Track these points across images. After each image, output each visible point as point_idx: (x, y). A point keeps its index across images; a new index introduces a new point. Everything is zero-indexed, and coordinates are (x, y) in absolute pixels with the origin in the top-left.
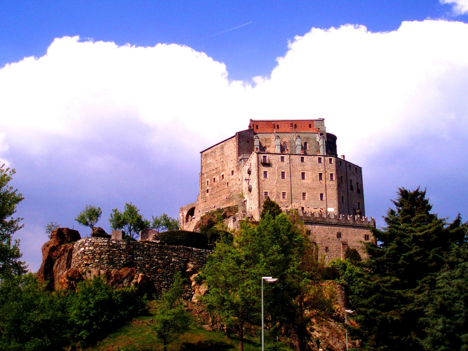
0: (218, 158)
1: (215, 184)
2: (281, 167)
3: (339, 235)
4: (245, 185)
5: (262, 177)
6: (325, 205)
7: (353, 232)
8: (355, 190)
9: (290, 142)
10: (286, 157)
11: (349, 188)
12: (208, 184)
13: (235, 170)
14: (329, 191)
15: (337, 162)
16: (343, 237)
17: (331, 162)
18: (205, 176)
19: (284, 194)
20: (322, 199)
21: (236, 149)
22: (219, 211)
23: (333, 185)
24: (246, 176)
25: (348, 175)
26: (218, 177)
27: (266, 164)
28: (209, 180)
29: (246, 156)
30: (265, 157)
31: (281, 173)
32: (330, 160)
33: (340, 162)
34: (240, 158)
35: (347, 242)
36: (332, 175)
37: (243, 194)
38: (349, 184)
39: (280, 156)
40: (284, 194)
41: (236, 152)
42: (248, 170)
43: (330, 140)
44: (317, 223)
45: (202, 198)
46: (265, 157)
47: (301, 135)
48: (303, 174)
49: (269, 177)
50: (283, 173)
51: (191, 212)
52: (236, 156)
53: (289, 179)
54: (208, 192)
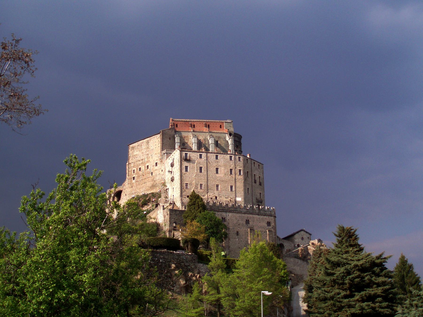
0: (144, 151)
1: (141, 173)
2: (199, 163)
3: (247, 222)
4: (168, 177)
5: (184, 171)
6: (234, 195)
7: (258, 219)
8: (258, 183)
10: (204, 155)
11: (253, 181)
12: (134, 172)
13: (158, 162)
14: (238, 184)
15: (244, 160)
17: (239, 160)
18: (132, 165)
19: (201, 185)
20: (231, 190)
21: (160, 145)
22: (145, 196)
23: (240, 178)
24: (169, 168)
25: (253, 171)
26: (143, 167)
27: (187, 160)
28: (135, 169)
29: (168, 151)
30: (186, 154)
31: (199, 168)
32: (239, 158)
33: (247, 160)
34: (163, 152)
35: (253, 228)
37: (165, 183)
38: (253, 178)
39: (199, 154)
40: (201, 185)
41: (160, 147)
42: (171, 164)
43: (237, 139)
44: (230, 212)
45: (128, 184)
46: (186, 154)
48: (217, 169)
49: (189, 170)
52: (159, 151)
53: (206, 173)
54: (134, 179)
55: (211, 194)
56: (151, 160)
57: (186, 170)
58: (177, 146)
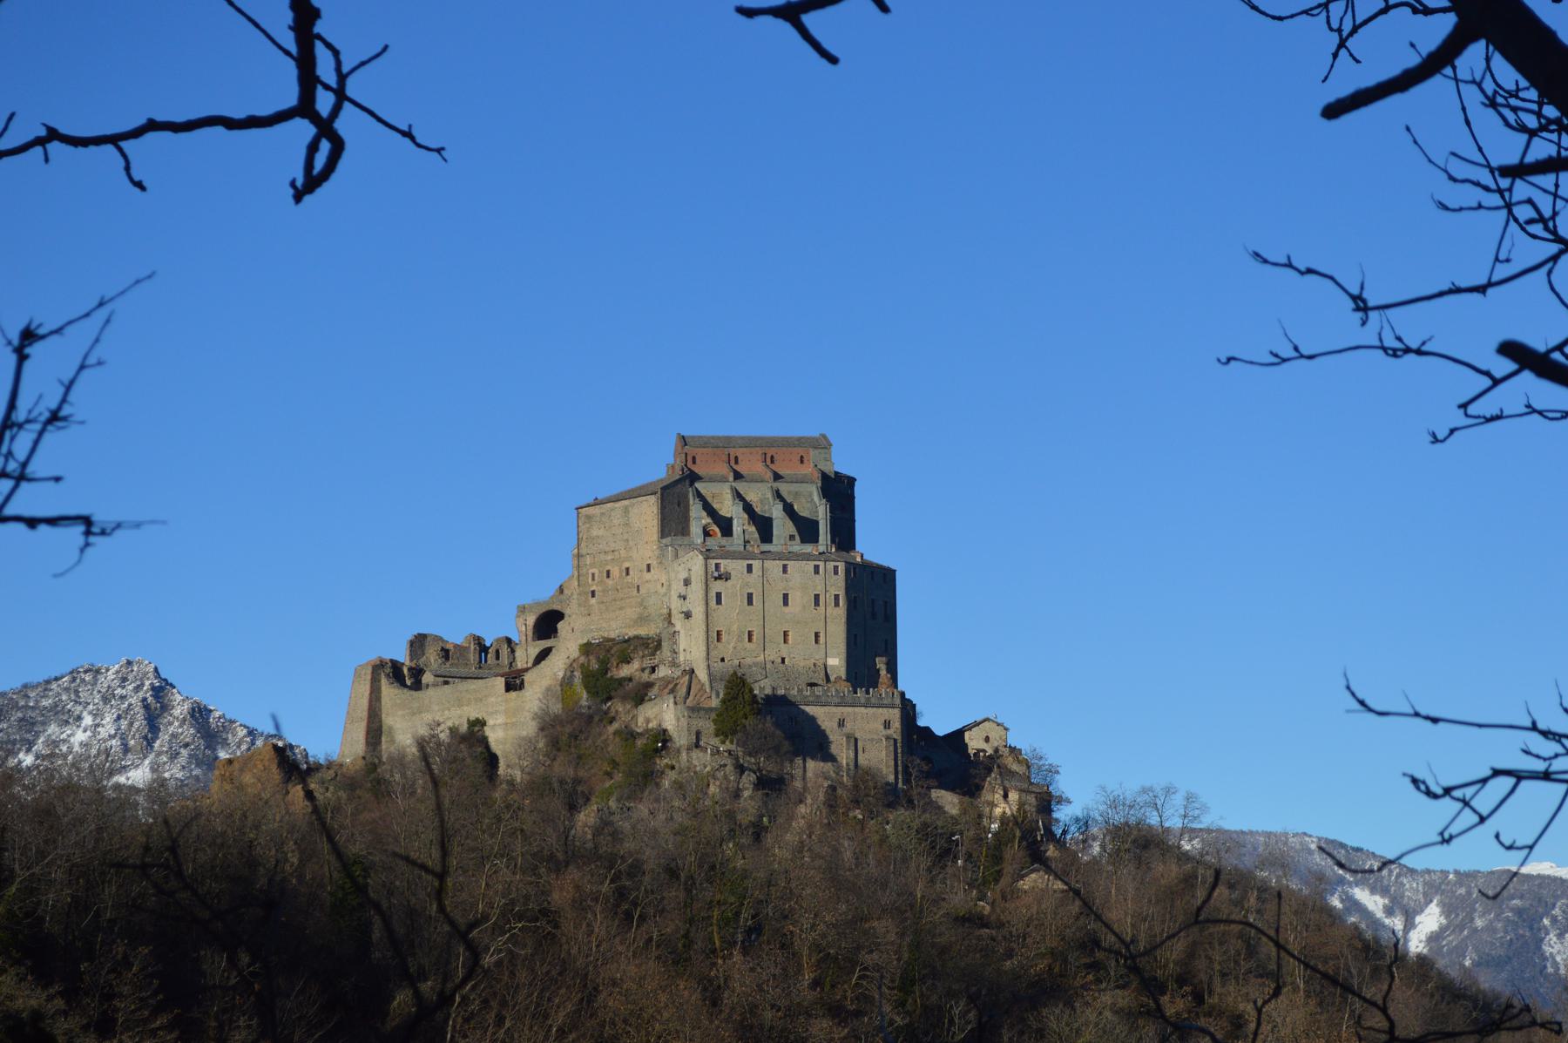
1: (610, 582)
9: (761, 501)
10: (756, 564)
16: (849, 727)
17: (836, 573)
18: (588, 560)
19: (750, 634)
20: (817, 641)
30: (717, 566)
32: (836, 568)
36: (837, 597)
37: (670, 614)
40: (750, 634)
46: (717, 566)
47: (784, 488)
48: (786, 597)
50: (750, 596)
51: (548, 624)
55: (772, 654)
56: (634, 555)
57: (719, 601)
58: (696, 530)
